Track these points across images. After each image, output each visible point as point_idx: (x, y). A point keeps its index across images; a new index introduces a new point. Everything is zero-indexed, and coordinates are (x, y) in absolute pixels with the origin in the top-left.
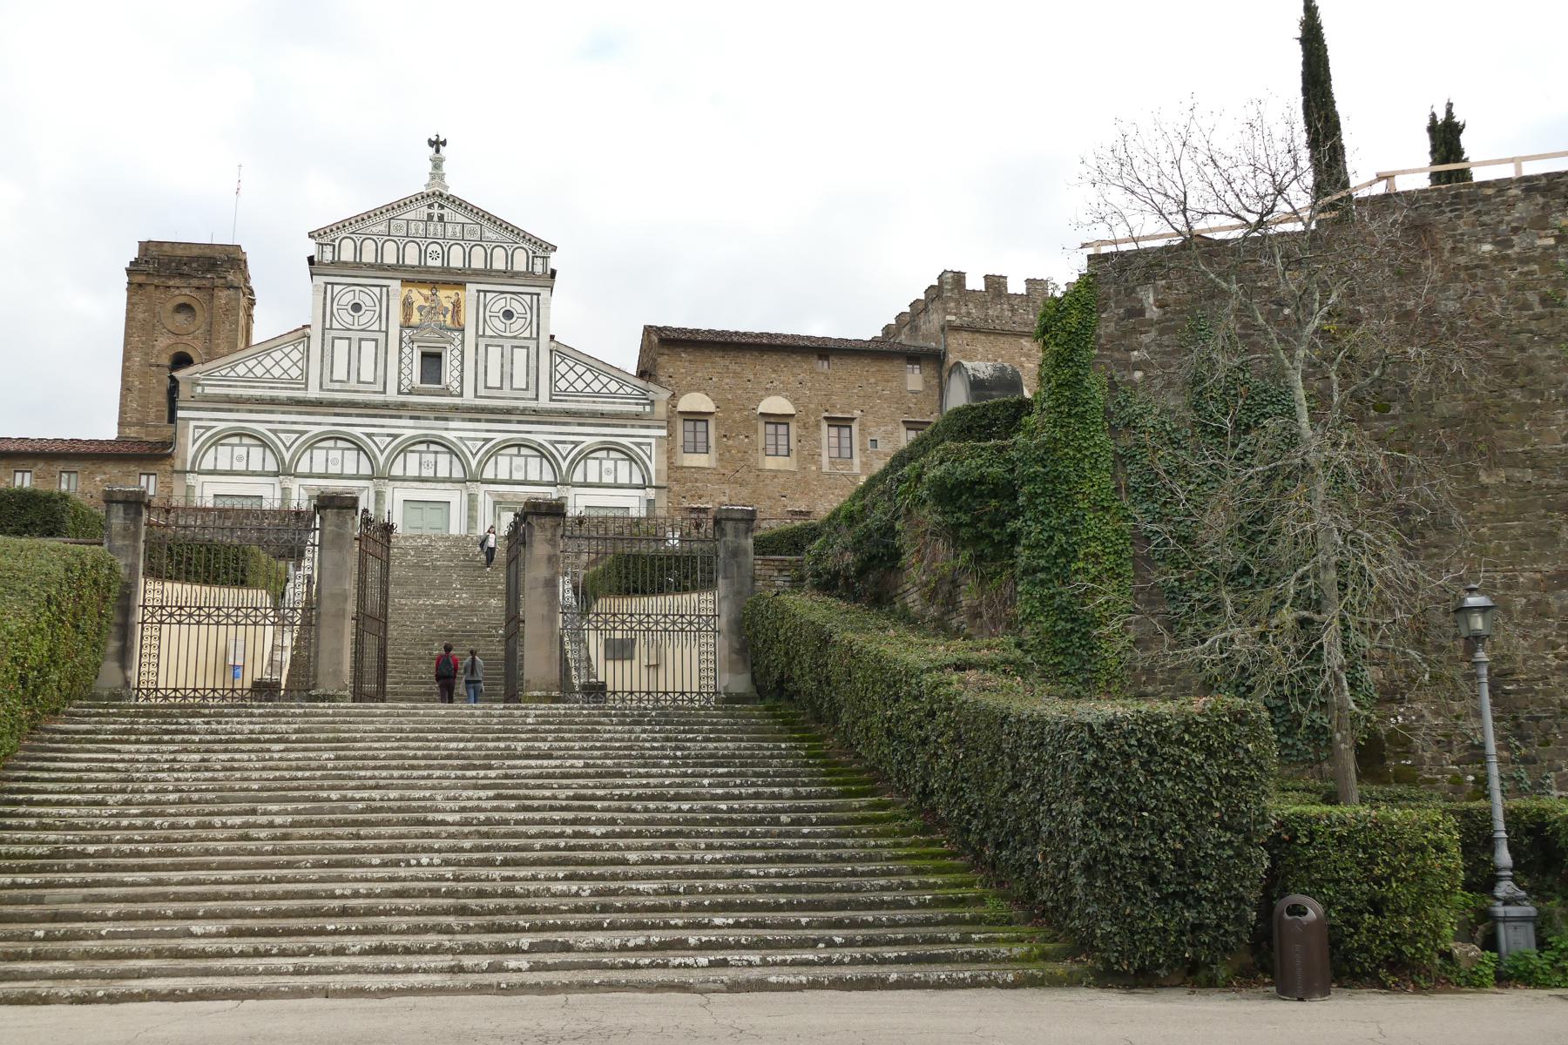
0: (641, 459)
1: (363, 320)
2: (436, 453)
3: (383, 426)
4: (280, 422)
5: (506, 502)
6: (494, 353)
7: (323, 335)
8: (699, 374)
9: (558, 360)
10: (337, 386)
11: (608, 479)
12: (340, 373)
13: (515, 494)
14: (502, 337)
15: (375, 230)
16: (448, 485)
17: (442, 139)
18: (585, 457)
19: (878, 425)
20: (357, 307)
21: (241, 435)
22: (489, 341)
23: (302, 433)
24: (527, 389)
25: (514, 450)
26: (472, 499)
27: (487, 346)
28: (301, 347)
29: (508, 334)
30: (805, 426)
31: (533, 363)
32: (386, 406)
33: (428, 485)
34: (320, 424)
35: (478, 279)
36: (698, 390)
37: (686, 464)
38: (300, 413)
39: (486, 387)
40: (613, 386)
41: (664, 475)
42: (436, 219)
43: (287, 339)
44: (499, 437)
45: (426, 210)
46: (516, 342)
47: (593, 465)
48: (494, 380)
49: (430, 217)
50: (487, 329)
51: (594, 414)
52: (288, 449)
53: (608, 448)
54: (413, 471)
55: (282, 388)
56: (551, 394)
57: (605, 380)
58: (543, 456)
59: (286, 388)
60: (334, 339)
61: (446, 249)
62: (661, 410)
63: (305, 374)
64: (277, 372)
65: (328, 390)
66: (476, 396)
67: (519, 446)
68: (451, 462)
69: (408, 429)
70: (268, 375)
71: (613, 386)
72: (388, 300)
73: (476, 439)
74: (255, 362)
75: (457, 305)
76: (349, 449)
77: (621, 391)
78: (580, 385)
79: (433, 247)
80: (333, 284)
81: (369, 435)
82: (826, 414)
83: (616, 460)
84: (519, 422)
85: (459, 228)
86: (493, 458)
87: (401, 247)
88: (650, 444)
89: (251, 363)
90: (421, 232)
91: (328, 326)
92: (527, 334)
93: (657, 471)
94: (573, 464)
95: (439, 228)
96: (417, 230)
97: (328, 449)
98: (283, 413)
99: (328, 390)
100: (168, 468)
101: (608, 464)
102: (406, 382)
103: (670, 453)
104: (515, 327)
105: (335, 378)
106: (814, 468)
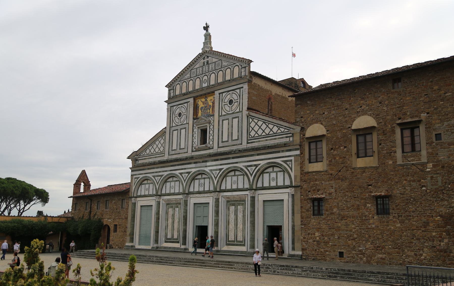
0: (287, 170)
2: (204, 178)
3: (185, 169)
6: (226, 122)
8: (317, 112)
9: (251, 120)
10: (173, 152)
11: (273, 184)
13: (234, 196)
14: (228, 114)
15: (186, 77)
16: (208, 195)
18: (263, 173)
19: (442, 121)
20: (180, 115)
21: (147, 180)
23: (162, 176)
24: (238, 140)
25: (232, 173)
26: (217, 200)
27: (223, 120)
28: (164, 138)
29: (231, 112)
30: (384, 133)
31: (240, 124)
32: (186, 159)
33: (202, 195)
35: (219, 88)
36: (317, 122)
37: (310, 170)
38: (161, 167)
39: (222, 142)
41: (298, 179)
42: (206, 64)
43: (159, 135)
44: (225, 167)
45: (202, 61)
46: (234, 115)
47: (266, 176)
48: (225, 139)
50: (223, 111)
51: (265, 148)
53: (273, 165)
54: (196, 190)
56: (248, 140)
57: (271, 126)
61: (209, 77)
62: (297, 139)
64: (157, 150)
66: (218, 147)
67: (235, 170)
69: (193, 169)
71: (275, 129)
73: (216, 170)
74: (151, 147)
75: (213, 103)
76: (177, 181)
77: (279, 131)
78: (260, 132)
79: (206, 78)
80: (173, 106)
81: (181, 174)
82: (399, 121)
83: (277, 172)
86: (225, 179)
87: (194, 81)
88: (291, 161)
89: (150, 148)
91: (171, 126)
92: (238, 110)
93: (295, 176)
96: (199, 71)
100: (128, 196)
101: (273, 175)
102: (194, 146)
103: (302, 165)
104: (233, 108)
105: (173, 149)
106: (391, 162)
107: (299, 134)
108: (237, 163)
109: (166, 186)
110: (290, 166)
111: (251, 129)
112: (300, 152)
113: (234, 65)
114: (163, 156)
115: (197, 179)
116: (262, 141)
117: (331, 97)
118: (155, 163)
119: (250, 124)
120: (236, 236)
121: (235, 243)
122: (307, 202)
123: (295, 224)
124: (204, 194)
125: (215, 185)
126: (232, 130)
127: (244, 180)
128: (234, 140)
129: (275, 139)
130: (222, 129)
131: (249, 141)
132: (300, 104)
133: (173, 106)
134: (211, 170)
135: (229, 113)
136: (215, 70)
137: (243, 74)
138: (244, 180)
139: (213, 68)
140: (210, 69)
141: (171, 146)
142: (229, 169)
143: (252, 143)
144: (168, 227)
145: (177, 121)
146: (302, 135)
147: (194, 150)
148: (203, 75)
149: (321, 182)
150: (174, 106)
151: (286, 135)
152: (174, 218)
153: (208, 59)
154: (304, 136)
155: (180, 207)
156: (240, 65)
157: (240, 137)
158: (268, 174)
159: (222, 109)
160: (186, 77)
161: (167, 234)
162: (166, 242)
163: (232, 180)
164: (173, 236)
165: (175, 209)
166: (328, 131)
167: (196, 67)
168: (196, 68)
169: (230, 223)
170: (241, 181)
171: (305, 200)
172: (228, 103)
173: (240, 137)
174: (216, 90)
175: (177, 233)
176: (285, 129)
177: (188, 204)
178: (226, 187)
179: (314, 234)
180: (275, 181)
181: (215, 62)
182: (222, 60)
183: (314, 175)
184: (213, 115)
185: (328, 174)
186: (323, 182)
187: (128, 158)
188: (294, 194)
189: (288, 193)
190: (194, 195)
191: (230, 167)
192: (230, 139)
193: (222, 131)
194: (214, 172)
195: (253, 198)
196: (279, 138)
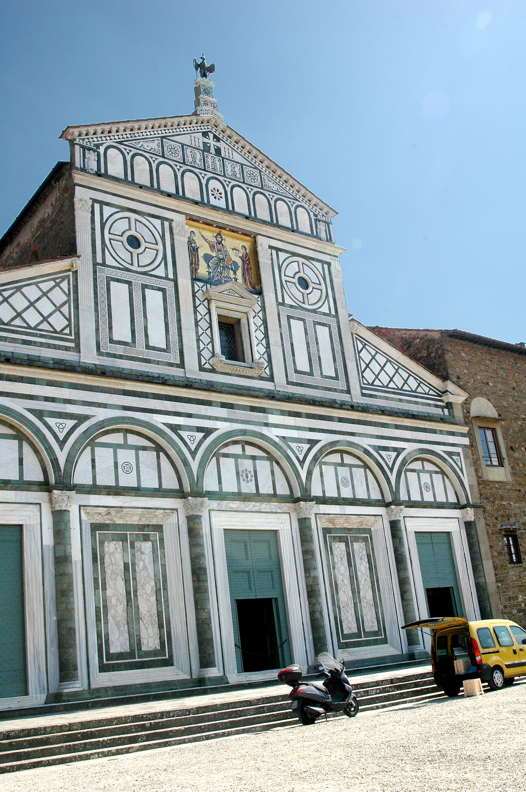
1: (145, 259)
2: (254, 458)
3: (190, 416)
4: (47, 399)
5: (336, 530)
6: (297, 326)
7: (95, 272)
10: (119, 350)
16: (274, 506)
17: (207, 65)
23: (81, 419)
28: (64, 285)
33: (251, 505)
34: (105, 406)
40: (413, 383)
42: (212, 150)
44: (325, 439)
48: (303, 365)
49: (206, 148)
50: (286, 297)
52: (62, 444)
55: (41, 345)
58: (366, 466)
59: (49, 346)
60: (109, 280)
62: (458, 413)
64: (32, 317)
65: (109, 355)
66: (288, 383)
67: (342, 452)
68: (272, 472)
70: (18, 322)
71: (413, 383)
73: (299, 440)
76: (144, 448)
77: (420, 390)
79: (213, 184)
80: (102, 203)
81: (175, 428)
83: (431, 473)
84: (341, 420)
85: (237, 169)
88: (458, 454)
90: (199, 163)
92: (325, 309)
93: (471, 486)
95: (217, 162)
96: (194, 158)
97: (116, 447)
98: (51, 383)
99: (109, 355)
102: (206, 354)
105: (116, 338)
107: (460, 407)
108: (353, 434)
109: (93, 461)
110: (459, 464)
112: (470, 442)
113: (297, 203)
114: (67, 349)
115: (226, 455)
116: (392, 399)
117: (491, 361)
118: (38, 364)
119: (359, 352)
120: (359, 620)
121: (363, 639)
122: (496, 537)
123: (487, 581)
124: (258, 504)
125: (304, 481)
126: (318, 350)
127: (367, 480)
129: (416, 403)
130: (291, 338)
131: (364, 391)
132: (452, 352)
134: (284, 437)
135: (303, 305)
136: (244, 183)
138: (367, 480)
139: (238, 176)
142: (335, 446)
143: (371, 396)
144: (111, 612)
145: (126, 256)
146: (465, 411)
147: (207, 366)
149: (509, 502)
150: (108, 204)
151: (435, 402)
152: (134, 579)
153: (218, 144)
154: (468, 414)
155: (162, 540)
156: (311, 211)
158: (416, 473)
159: (282, 289)
160: (145, 145)
161: (107, 641)
162: (103, 668)
163: (337, 475)
164: (139, 644)
165: (137, 544)
166: (500, 415)
168: (183, 145)
169: (339, 587)
170: (362, 482)
171: (492, 534)
173: (341, 374)
174: (260, 235)
175: (156, 630)
176: (431, 389)
177: (205, 529)
178: (324, 492)
179: (517, 598)
180: (431, 491)
181: (242, 165)
182: (260, 171)
183: (497, 488)
185: (516, 490)
186: (512, 503)
188: (474, 522)
189: (458, 518)
190: (224, 503)
191: (337, 442)
193: (292, 344)
194: (293, 445)
195: (394, 526)
196: (423, 404)
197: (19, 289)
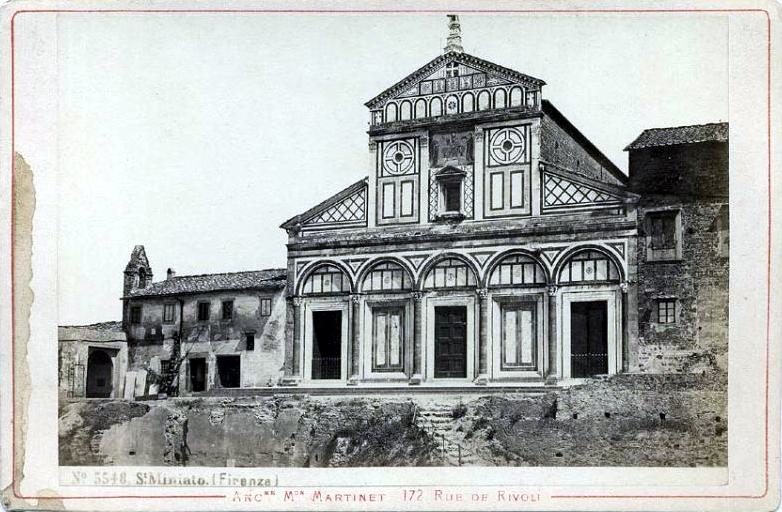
2: (456, 267)
9: (547, 178)
10: (387, 221)
11: (589, 277)
12: (389, 212)
14: (502, 165)
22: (493, 170)
27: (492, 174)
31: (527, 185)
39: (491, 209)
42: (453, 75)
46: (515, 168)
48: (497, 203)
56: (542, 209)
57: (586, 191)
61: (460, 99)
63: (366, 213)
64: (348, 215)
70: (342, 219)
72: (420, 150)
74: (334, 209)
78: (565, 198)
81: (407, 258)
88: (623, 244)
91: (380, 175)
92: (522, 160)
94: (559, 269)
96: (439, 86)
111: (547, 192)
128: (515, 208)
133: (382, 142)
135: (504, 162)
137: (531, 102)
140: (463, 86)
141: (380, 212)
144: (378, 348)
148: (448, 94)
150: (387, 141)
153: (456, 68)
157: (527, 203)
160: (410, 93)
162: (373, 371)
167: (432, 77)
168: (432, 81)
172: (501, 147)
173: (527, 203)
178: (500, 280)
184: (473, 164)
187: (281, 227)
192: (507, 207)
197: (342, 203)
